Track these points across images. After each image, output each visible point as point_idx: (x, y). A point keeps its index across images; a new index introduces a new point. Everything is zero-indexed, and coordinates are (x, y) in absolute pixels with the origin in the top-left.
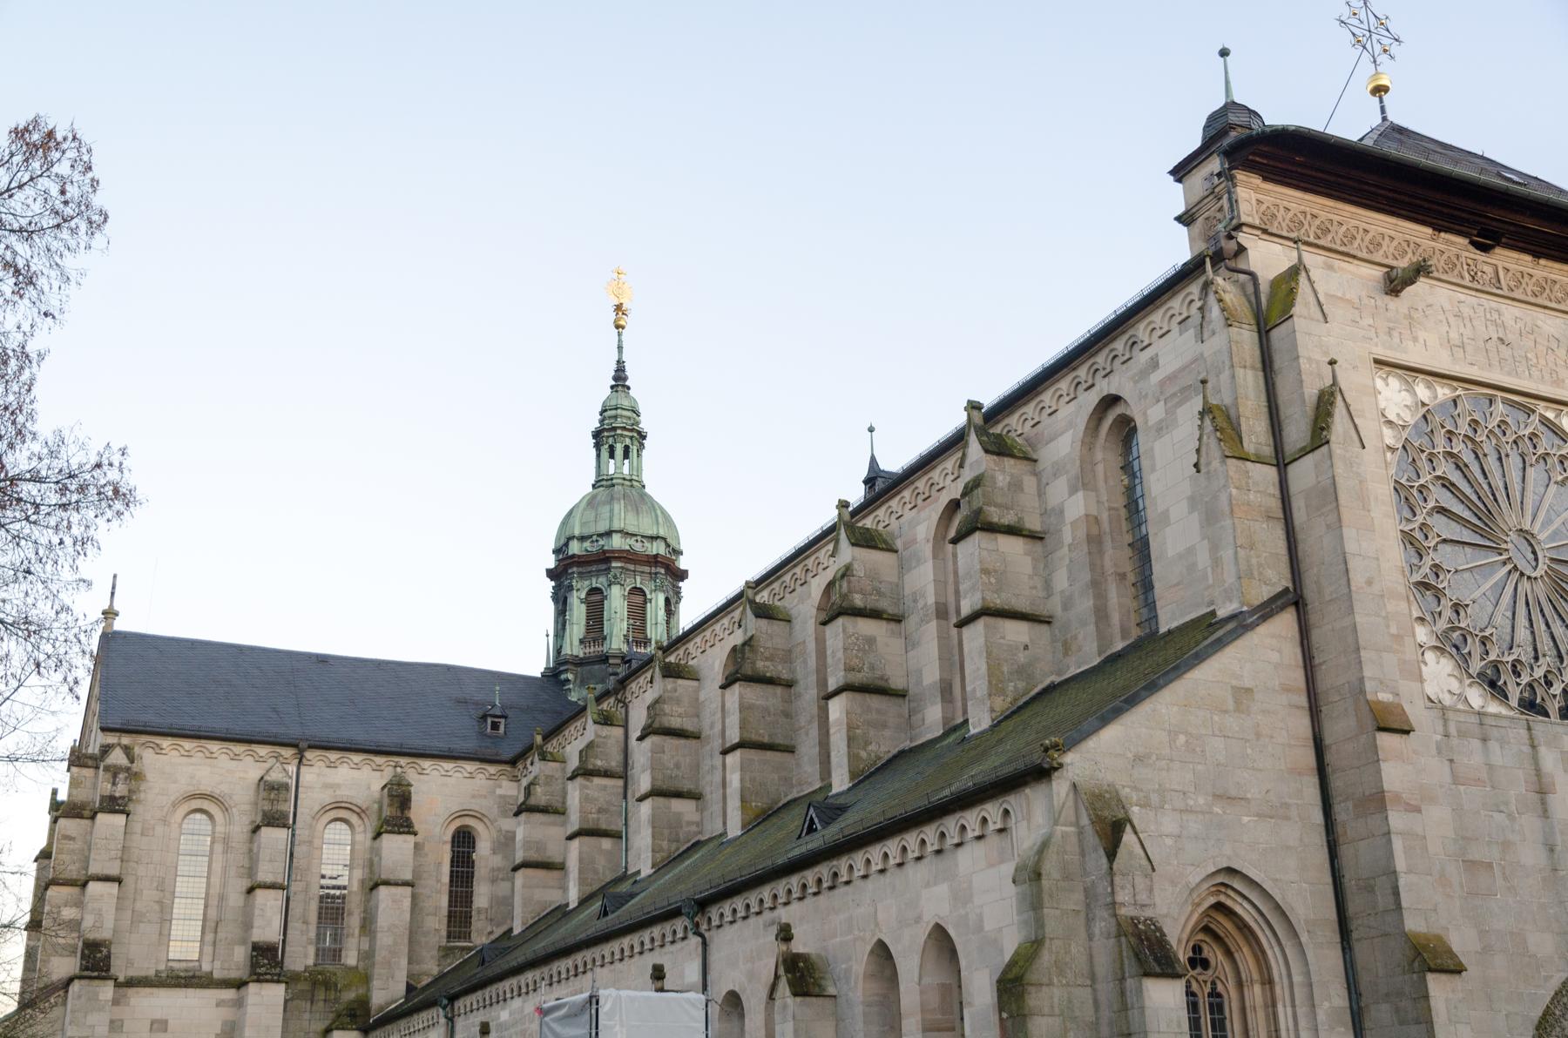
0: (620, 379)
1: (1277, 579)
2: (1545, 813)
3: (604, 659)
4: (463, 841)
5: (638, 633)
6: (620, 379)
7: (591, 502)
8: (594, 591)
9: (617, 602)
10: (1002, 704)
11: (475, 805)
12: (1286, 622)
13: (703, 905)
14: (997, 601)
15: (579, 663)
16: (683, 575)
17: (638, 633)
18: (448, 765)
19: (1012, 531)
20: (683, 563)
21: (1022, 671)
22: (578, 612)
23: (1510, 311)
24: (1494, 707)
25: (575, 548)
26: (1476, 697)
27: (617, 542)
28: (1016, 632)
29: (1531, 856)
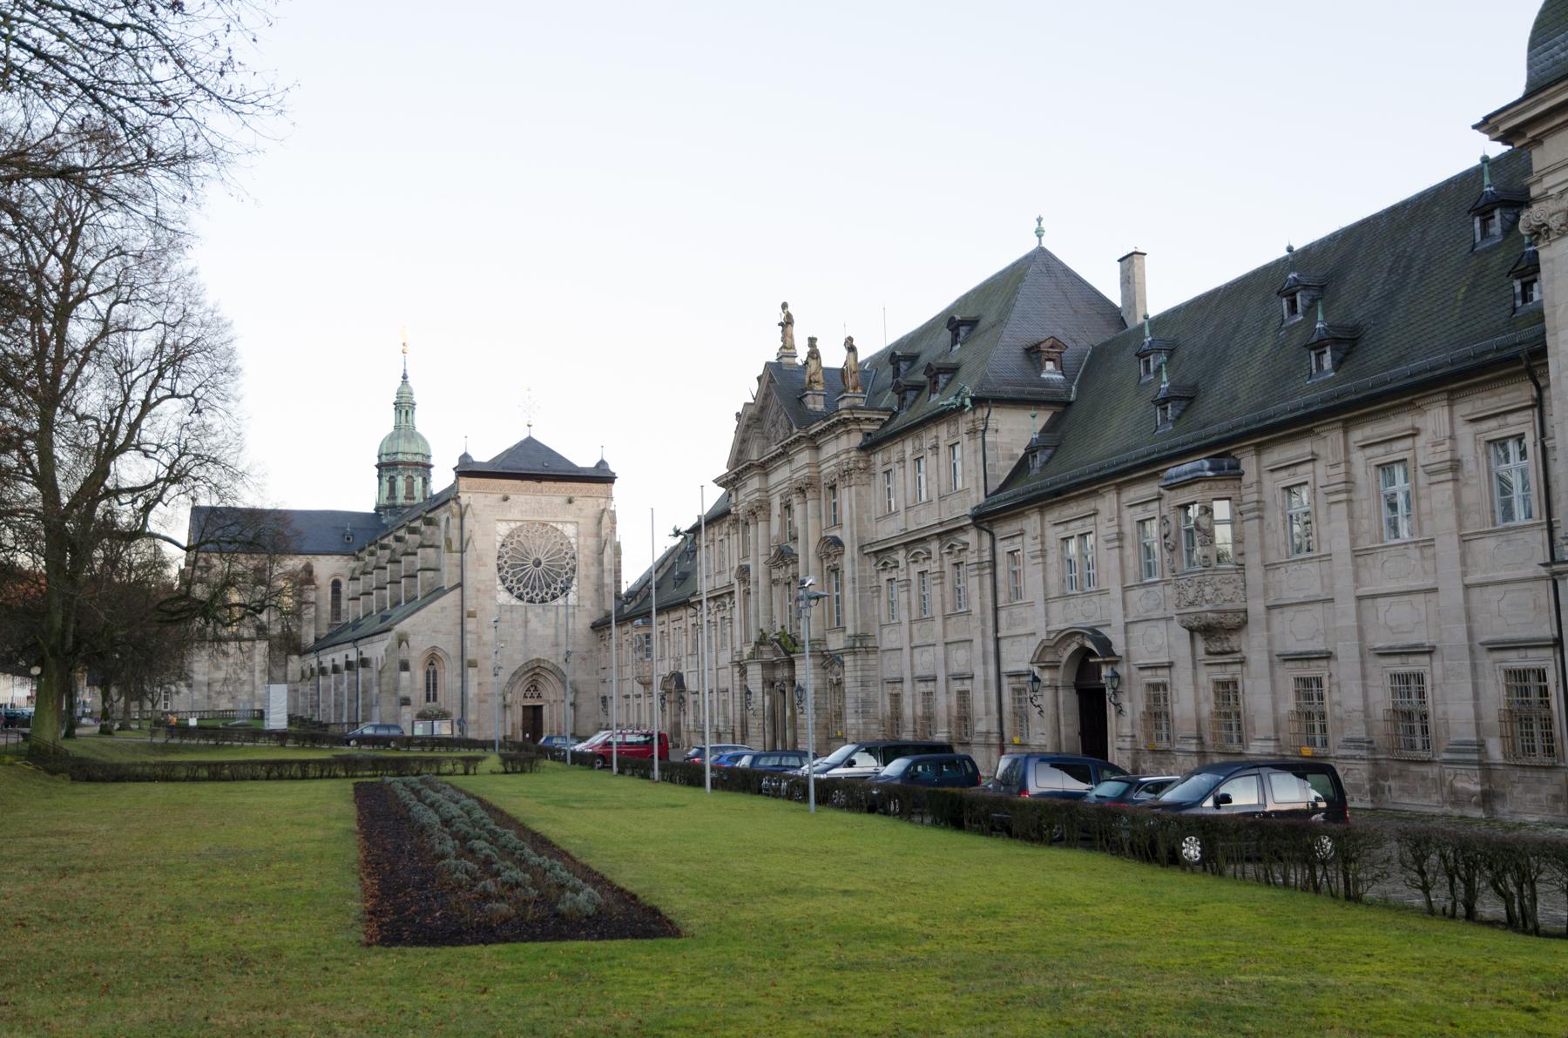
0: (405, 377)
1: (457, 581)
2: (526, 627)
3: (394, 506)
4: (336, 585)
5: (410, 495)
6: (405, 377)
7: (391, 437)
8: (391, 477)
9: (401, 483)
10: (424, 593)
11: (340, 571)
12: (458, 590)
13: (357, 640)
14: (425, 566)
15: (386, 507)
16: (431, 466)
17: (410, 495)
18: (328, 557)
19: (431, 546)
20: (433, 461)
21: (430, 585)
22: (386, 485)
23: (544, 499)
24: (520, 603)
25: (384, 459)
26: (514, 601)
27: (400, 457)
28: (429, 574)
29: (520, 637)
